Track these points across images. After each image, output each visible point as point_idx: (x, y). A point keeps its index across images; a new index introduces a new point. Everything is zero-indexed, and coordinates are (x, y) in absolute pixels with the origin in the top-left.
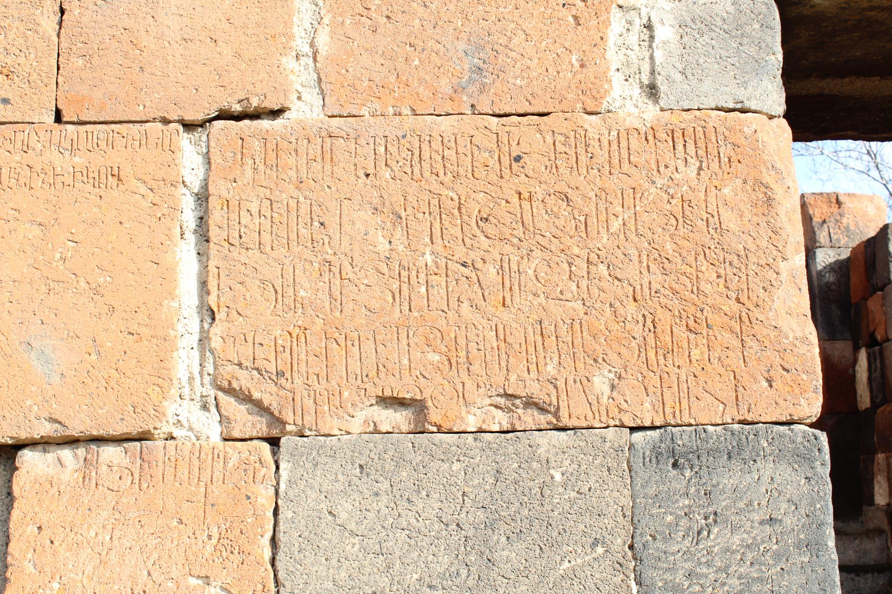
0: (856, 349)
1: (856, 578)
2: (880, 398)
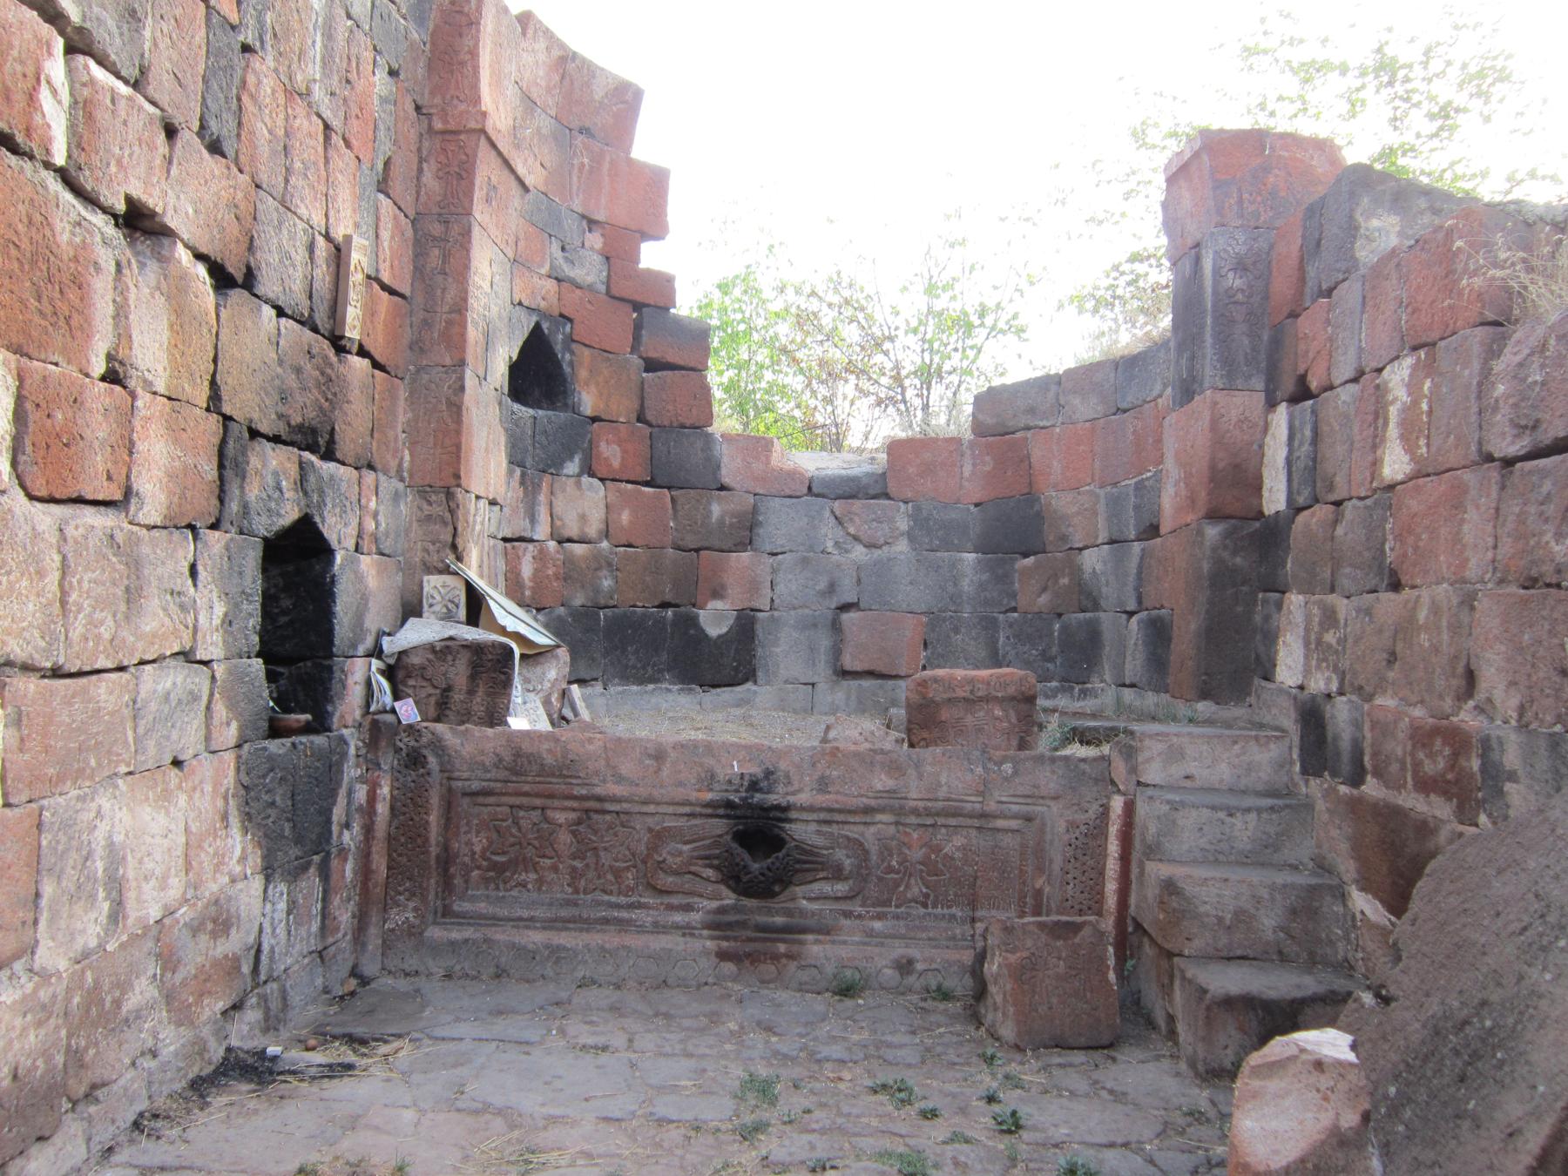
0: (1271, 405)
1: (1229, 820)
2: (1306, 492)
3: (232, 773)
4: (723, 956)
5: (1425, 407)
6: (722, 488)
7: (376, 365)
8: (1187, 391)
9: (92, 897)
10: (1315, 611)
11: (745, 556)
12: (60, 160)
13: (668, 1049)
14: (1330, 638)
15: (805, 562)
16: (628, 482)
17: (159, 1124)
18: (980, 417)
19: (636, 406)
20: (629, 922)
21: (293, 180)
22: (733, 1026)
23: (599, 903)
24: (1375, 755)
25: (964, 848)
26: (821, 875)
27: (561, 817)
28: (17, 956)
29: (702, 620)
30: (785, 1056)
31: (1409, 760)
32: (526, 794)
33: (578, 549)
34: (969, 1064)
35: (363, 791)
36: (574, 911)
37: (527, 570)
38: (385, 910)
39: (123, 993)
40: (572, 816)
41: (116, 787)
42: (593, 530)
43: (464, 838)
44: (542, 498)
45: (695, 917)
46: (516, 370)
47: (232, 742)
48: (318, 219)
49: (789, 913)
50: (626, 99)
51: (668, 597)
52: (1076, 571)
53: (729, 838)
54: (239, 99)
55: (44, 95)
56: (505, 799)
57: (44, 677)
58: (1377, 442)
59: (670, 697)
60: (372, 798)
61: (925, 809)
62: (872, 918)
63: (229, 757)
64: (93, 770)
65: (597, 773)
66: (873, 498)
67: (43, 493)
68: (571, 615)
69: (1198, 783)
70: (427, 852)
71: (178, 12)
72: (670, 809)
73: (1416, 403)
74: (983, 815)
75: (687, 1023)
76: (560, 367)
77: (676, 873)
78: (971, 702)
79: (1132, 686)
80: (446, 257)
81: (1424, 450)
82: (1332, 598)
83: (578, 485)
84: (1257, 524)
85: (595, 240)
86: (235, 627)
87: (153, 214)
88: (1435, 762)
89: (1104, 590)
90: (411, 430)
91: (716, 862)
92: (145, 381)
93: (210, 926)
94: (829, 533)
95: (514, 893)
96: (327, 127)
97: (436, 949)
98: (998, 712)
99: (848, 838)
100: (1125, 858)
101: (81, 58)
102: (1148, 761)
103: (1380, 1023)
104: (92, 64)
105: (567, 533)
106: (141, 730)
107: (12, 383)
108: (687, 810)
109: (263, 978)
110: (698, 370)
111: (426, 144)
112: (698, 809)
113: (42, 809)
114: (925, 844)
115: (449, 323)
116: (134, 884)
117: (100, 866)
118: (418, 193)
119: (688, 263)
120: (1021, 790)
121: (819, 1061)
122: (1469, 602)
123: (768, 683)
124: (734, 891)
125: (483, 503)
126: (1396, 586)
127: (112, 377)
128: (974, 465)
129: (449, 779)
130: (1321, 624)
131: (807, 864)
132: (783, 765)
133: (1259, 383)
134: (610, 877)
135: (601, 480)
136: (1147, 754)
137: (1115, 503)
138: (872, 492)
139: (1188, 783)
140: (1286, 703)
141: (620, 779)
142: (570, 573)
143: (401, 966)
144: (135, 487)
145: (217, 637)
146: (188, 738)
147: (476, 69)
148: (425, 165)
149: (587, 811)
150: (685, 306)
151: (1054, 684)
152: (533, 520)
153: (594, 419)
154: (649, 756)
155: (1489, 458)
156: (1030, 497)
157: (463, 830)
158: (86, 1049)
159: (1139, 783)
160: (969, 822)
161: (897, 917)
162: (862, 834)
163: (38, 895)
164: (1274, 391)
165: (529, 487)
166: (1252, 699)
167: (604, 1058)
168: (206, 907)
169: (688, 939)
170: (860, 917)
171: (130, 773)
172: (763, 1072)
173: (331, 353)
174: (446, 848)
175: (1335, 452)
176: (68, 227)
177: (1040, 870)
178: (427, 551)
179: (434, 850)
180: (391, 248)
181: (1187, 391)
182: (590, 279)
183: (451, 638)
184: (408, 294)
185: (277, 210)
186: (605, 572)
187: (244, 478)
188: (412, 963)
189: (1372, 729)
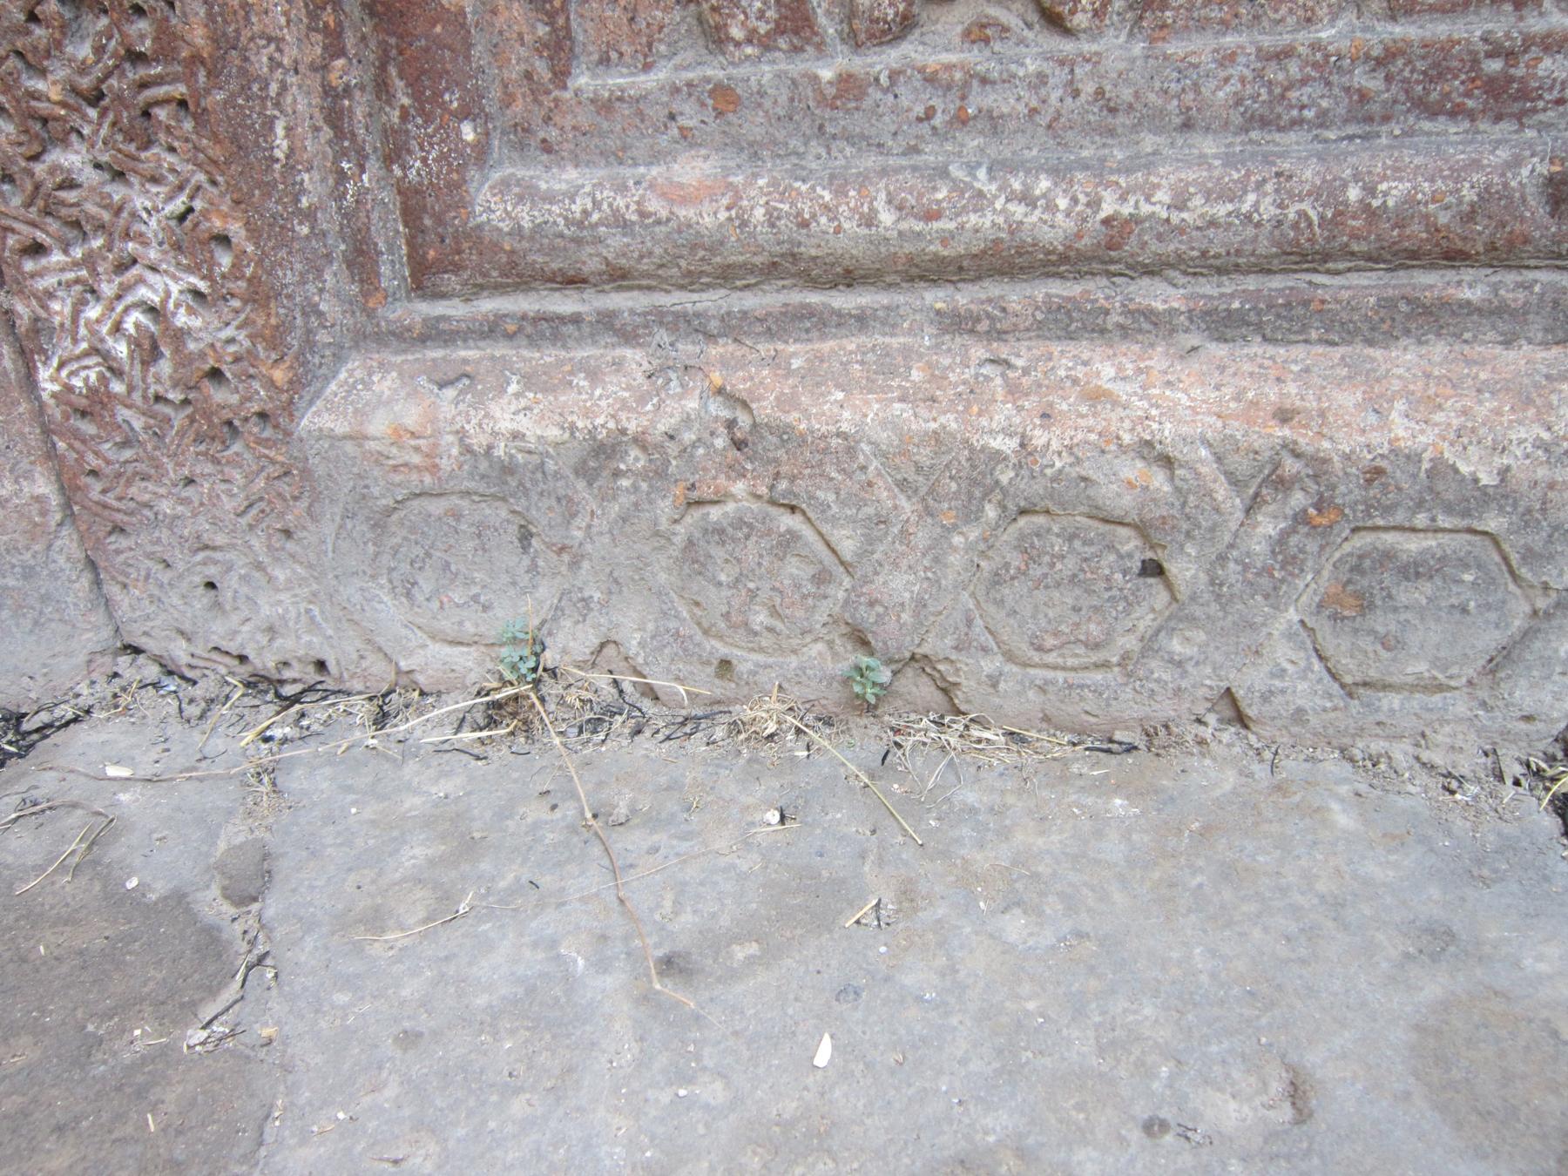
97: (404, 517)
143: (218, 631)
188: (277, 614)
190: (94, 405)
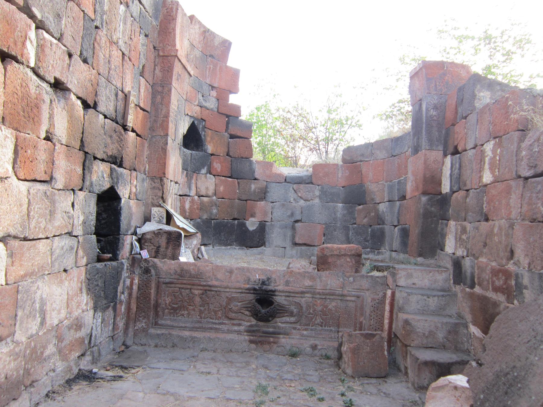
0: (445, 155)
1: (428, 299)
3: (84, 274)
4: (251, 342)
5: (498, 158)
6: (255, 179)
7: (138, 135)
8: (416, 150)
9: (35, 316)
10: (459, 227)
11: (263, 203)
12: (32, 65)
13: (231, 374)
14: (464, 237)
15: (283, 205)
16: (223, 176)
17: (55, 395)
18: (345, 157)
19: (226, 150)
20: (219, 329)
21: (111, 72)
22: (254, 366)
23: (209, 322)
24: (479, 278)
25: (335, 307)
26: (286, 314)
27: (196, 292)
28: (8, 336)
29: (247, 224)
30: (272, 378)
31: (490, 280)
32: (185, 284)
33: (205, 199)
34: (335, 382)
35: (129, 281)
36: (200, 325)
37: (187, 206)
38: (135, 323)
39: (44, 350)
40: (201, 292)
41: (44, 279)
42: (210, 193)
43: (163, 298)
44: (193, 181)
45: (242, 328)
46: (185, 137)
47: (84, 264)
48: (119, 85)
49: (275, 327)
50: (226, 45)
51: (236, 217)
52: (377, 211)
53: (254, 301)
54: (94, 45)
55: (28, 43)
56: (177, 285)
57: (21, 240)
58: (481, 170)
59: (236, 251)
60: (132, 283)
61: (323, 292)
62: (303, 330)
63: (83, 269)
64: (36, 273)
65: (209, 277)
66: (307, 184)
67: (23, 178)
68: (202, 222)
69: (417, 286)
70: (150, 303)
71: (74, 15)
72: (234, 290)
73: (495, 157)
74: (342, 295)
75: (238, 365)
76: (201, 137)
77: (236, 313)
78: (339, 256)
79: (395, 251)
80: (163, 98)
81: (497, 173)
82: (465, 223)
83: (206, 177)
84: (440, 197)
85: (214, 93)
86: (87, 224)
87: (63, 83)
88: (499, 281)
89: (386, 218)
90: (149, 157)
91: (250, 309)
92: (59, 140)
93: (75, 327)
94: (292, 196)
95: (180, 318)
96: (123, 54)
97: (152, 337)
98: (349, 260)
99: (296, 302)
100: (391, 311)
101: (41, 31)
102: (400, 278)
103: (478, 373)
104: (44, 32)
105: (202, 194)
106: (53, 259)
107: (14, 140)
108: (240, 291)
109: (92, 345)
110: (247, 138)
111: (157, 60)
112: (244, 291)
113: (18, 286)
114: (322, 305)
115: (163, 121)
116: (49, 312)
117: (38, 305)
118: (154, 77)
119: (246, 102)
120: (355, 287)
121: (283, 380)
122: (512, 226)
123: (269, 247)
124: (256, 319)
125: (173, 183)
126: (487, 220)
127: (47, 139)
128: (342, 173)
129: (158, 278)
130: (461, 232)
131: (280, 311)
132: (274, 276)
133: (441, 148)
134: (213, 313)
135: (214, 175)
136: (400, 275)
137: (391, 188)
138: (307, 182)
139: (414, 286)
140: (448, 259)
141: (217, 280)
142: (202, 207)
144: (54, 176)
145: (80, 228)
146: (69, 262)
147: (175, 35)
148: (156, 67)
149: (206, 290)
150: (244, 116)
151: (368, 250)
152: (190, 188)
153: (212, 155)
154: (228, 272)
155: (520, 177)
156: (361, 185)
157: (163, 295)
158: (31, 368)
159: (397, 286)
160: (337, 297)
161: (312, 330)
162: (300, 301)
163: (16, 315)
164: (446, 151)
165: (189, 178)
166: (437, 257)
167: (209, 376)
168: (74, 320)
169: (239, 335)
170: (299, 329)
171: (49, 274)
172: (264, 383)
173: (122, 131)
174: (157, 301)
175: (467, 174)
176: (35, 88)
177: (362, 315)
178: (153, 199)
179: (152, 302)
180: (144, 95)
181: (416, 150)
182: (212, 107)
183: (160, 229)
184: (149, 111)
185: (105, 82)
186: (214, 207)
187: (91, 173)
188: (144, 341)
189: (478, 269)
190: (137, 330)
